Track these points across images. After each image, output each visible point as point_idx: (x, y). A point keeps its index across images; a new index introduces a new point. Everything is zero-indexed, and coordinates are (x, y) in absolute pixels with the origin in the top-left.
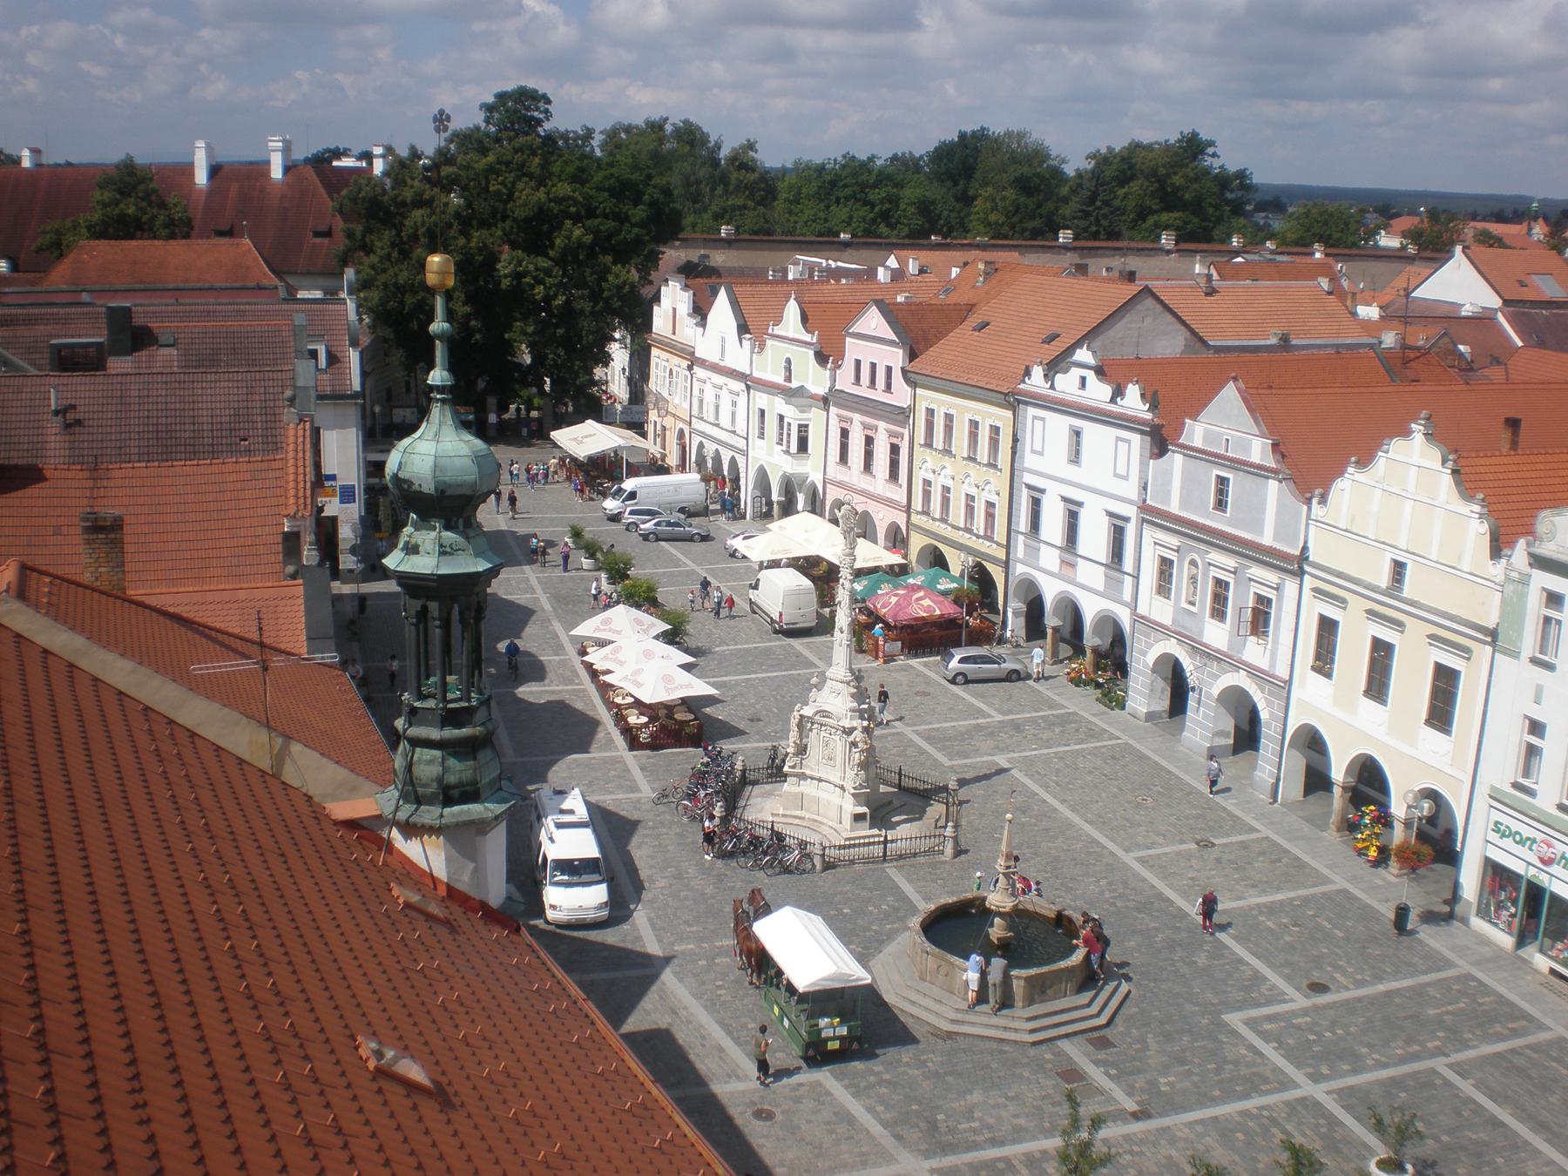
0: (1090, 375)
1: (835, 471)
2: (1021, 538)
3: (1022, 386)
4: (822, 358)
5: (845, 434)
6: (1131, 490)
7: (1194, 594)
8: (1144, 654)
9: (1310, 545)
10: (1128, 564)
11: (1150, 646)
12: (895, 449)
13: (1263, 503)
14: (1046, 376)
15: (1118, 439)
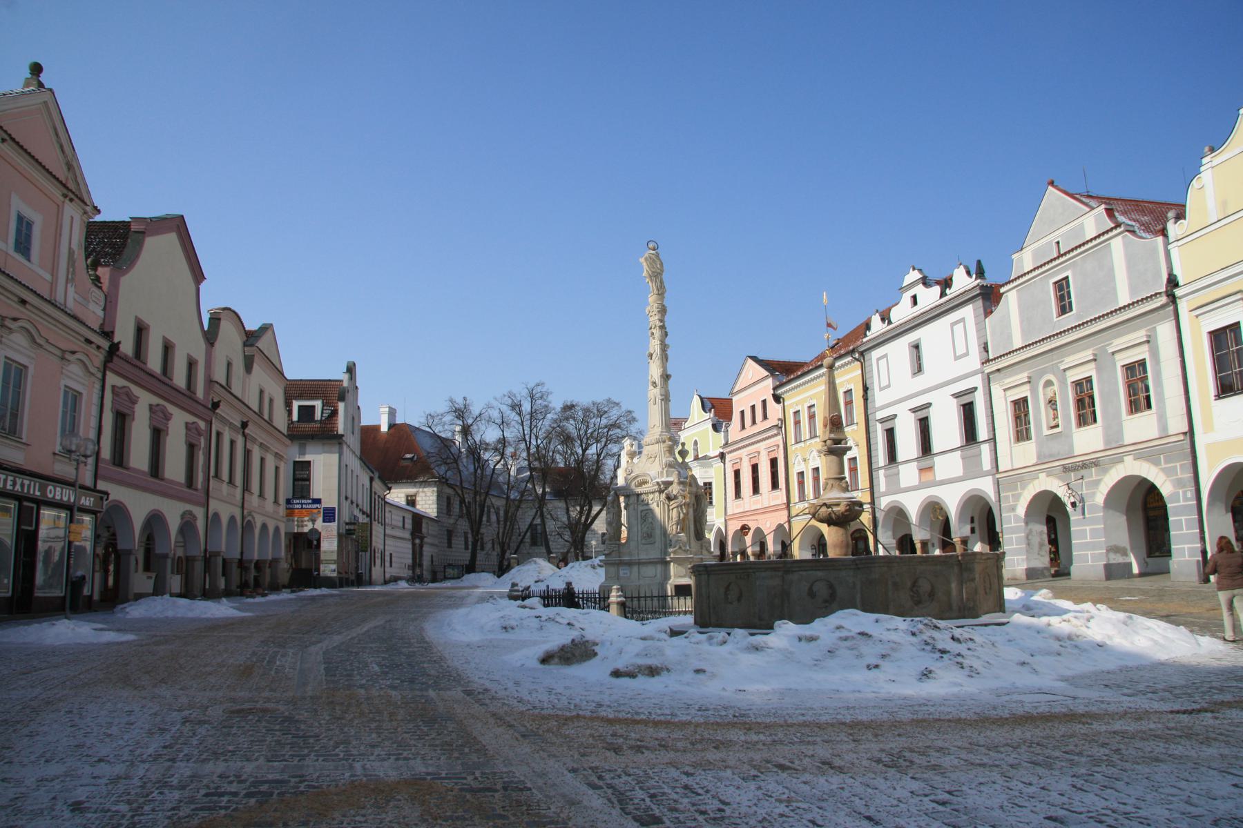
0: (920, 290)
1: (734, 507)
2: (881, 472)
3: (865, 340)
4: (716, 428)
5: (737, 474)
6: (974, 361)
7: (1055, 417)
8: (1013, 509)
9: (1177, 271)
10: (982, 432)
11: (1017, 498)
12: (774, 462)
13: (1112, 269)
14: (883, 320)
15: (953, 324)
